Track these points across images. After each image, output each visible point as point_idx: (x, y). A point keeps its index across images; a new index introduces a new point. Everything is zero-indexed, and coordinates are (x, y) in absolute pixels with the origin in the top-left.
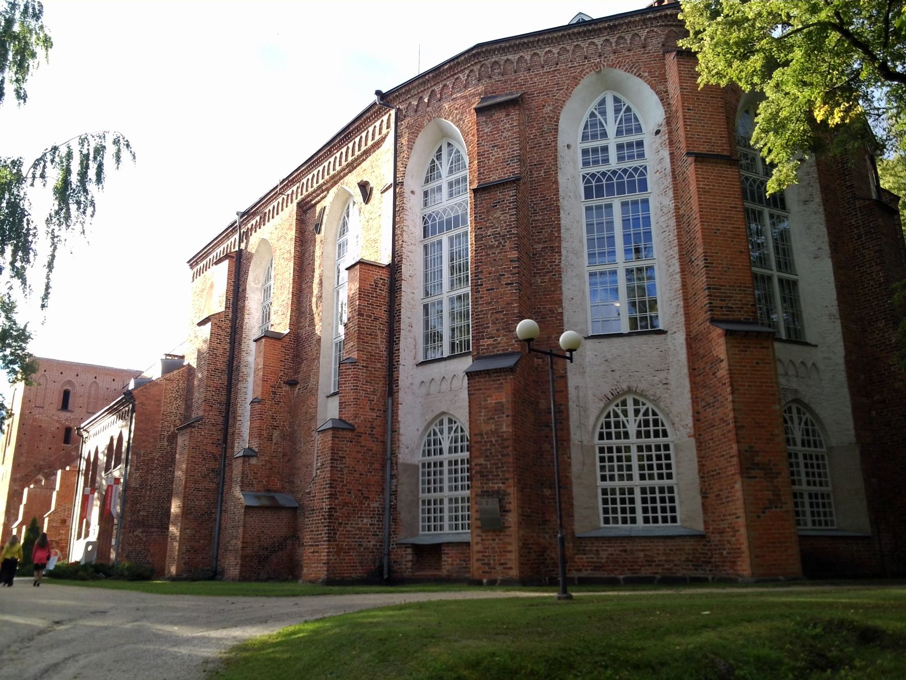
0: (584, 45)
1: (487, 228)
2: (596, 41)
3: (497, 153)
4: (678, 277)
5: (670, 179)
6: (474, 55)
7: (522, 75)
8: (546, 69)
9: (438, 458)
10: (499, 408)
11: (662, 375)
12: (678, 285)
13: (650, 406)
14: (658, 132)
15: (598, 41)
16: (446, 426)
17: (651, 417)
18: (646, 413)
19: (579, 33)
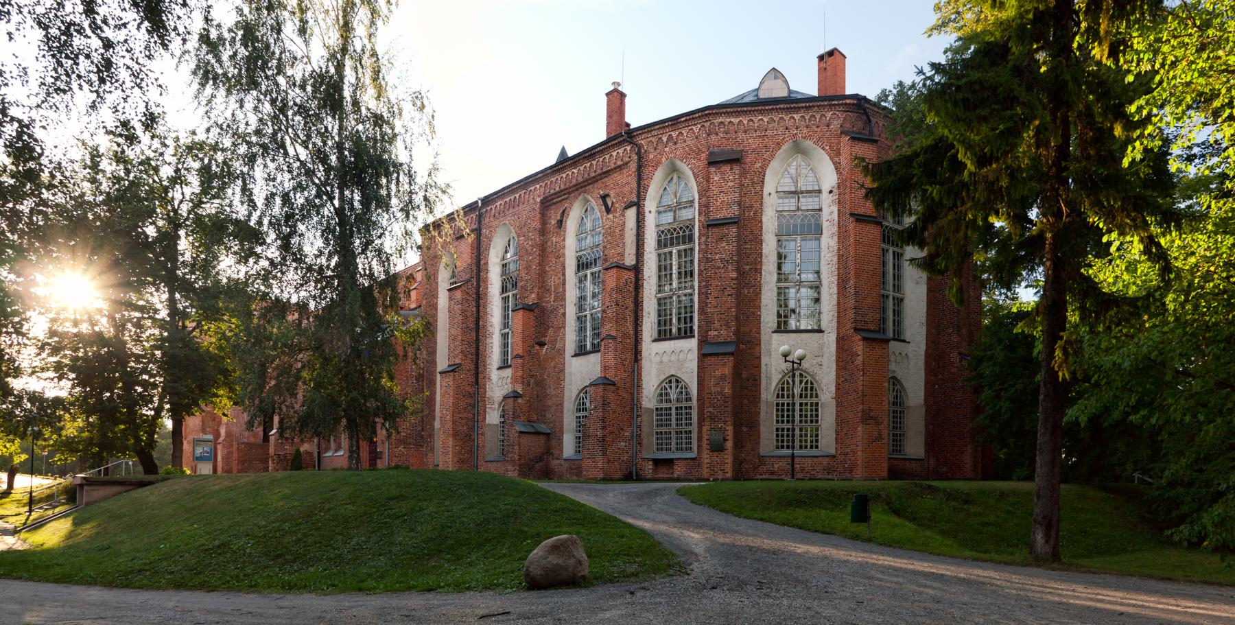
0: (787, 118)
1: (716, 253)
2: (795, 116)
3: (722, 198)
4: (835, 296)
5: (836, 229)
6: (706, 115)
7: (741, 135)
8: (758, 133)
9: (668, 405)
10: (723, 378)
11: (819, 359)
12: (835, 302)
13: (809, 378)
14: (831, 192)
15: (797, 117)
16: (674, 385)
17: (809, 385)
18: (807, 382)
19: (784, 109)
